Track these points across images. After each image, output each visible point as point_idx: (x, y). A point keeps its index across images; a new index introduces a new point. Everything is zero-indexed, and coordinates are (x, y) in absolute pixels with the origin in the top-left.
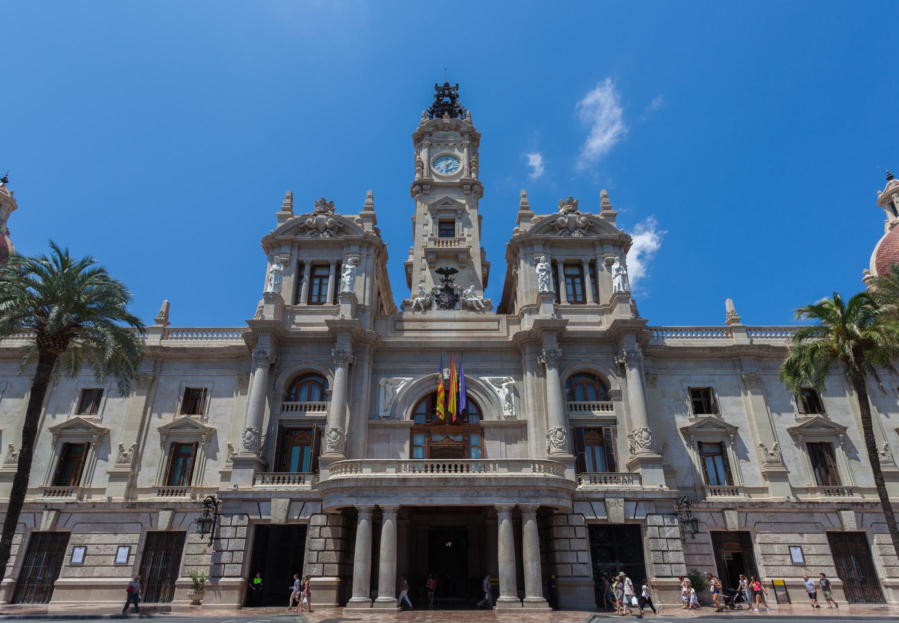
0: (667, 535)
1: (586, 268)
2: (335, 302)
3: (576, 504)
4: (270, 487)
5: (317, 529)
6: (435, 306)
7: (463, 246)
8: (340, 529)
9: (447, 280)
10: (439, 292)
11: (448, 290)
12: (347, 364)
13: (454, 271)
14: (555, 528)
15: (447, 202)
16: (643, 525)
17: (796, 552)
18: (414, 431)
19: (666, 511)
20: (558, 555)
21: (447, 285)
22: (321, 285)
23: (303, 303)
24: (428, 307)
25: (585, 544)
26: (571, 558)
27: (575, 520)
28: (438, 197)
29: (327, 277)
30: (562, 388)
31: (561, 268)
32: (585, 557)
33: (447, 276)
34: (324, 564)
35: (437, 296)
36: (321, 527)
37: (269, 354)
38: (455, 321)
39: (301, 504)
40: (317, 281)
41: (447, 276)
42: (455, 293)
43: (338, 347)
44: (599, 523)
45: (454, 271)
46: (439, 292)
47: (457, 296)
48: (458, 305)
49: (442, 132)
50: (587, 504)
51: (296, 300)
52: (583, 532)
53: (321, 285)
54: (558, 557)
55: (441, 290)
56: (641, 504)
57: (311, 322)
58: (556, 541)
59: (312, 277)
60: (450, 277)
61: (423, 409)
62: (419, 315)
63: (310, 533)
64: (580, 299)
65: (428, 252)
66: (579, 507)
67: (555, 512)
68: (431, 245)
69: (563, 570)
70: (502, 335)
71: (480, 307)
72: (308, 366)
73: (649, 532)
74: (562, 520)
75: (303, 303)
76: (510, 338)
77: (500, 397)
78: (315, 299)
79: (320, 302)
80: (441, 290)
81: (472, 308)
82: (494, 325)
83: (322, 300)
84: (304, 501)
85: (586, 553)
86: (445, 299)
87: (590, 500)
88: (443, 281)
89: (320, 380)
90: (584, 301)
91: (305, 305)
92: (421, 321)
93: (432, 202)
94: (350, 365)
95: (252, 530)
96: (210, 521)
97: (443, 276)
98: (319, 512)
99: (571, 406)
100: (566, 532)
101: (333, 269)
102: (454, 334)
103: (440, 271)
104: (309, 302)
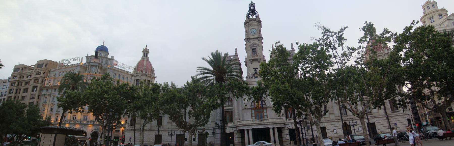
7: (259, 57)
13: (257, 68)
15: (254, 44)
17: (335, 131)
24: (252, 78)
25: (288, 133)
26: (285, 136)
27: (286, 128)
28: (252, 42)
32: (288, 136)
45: (257, 68)
49: (251, 22)
52: (288, 131)
61: (253, 104)
62: (250, 80)
65: (250, 60)
68: (251, 58)
74: (283, 129)
86: (256, 75)
93: (250, 44)
100: (284, 131)
103: (254, 69)
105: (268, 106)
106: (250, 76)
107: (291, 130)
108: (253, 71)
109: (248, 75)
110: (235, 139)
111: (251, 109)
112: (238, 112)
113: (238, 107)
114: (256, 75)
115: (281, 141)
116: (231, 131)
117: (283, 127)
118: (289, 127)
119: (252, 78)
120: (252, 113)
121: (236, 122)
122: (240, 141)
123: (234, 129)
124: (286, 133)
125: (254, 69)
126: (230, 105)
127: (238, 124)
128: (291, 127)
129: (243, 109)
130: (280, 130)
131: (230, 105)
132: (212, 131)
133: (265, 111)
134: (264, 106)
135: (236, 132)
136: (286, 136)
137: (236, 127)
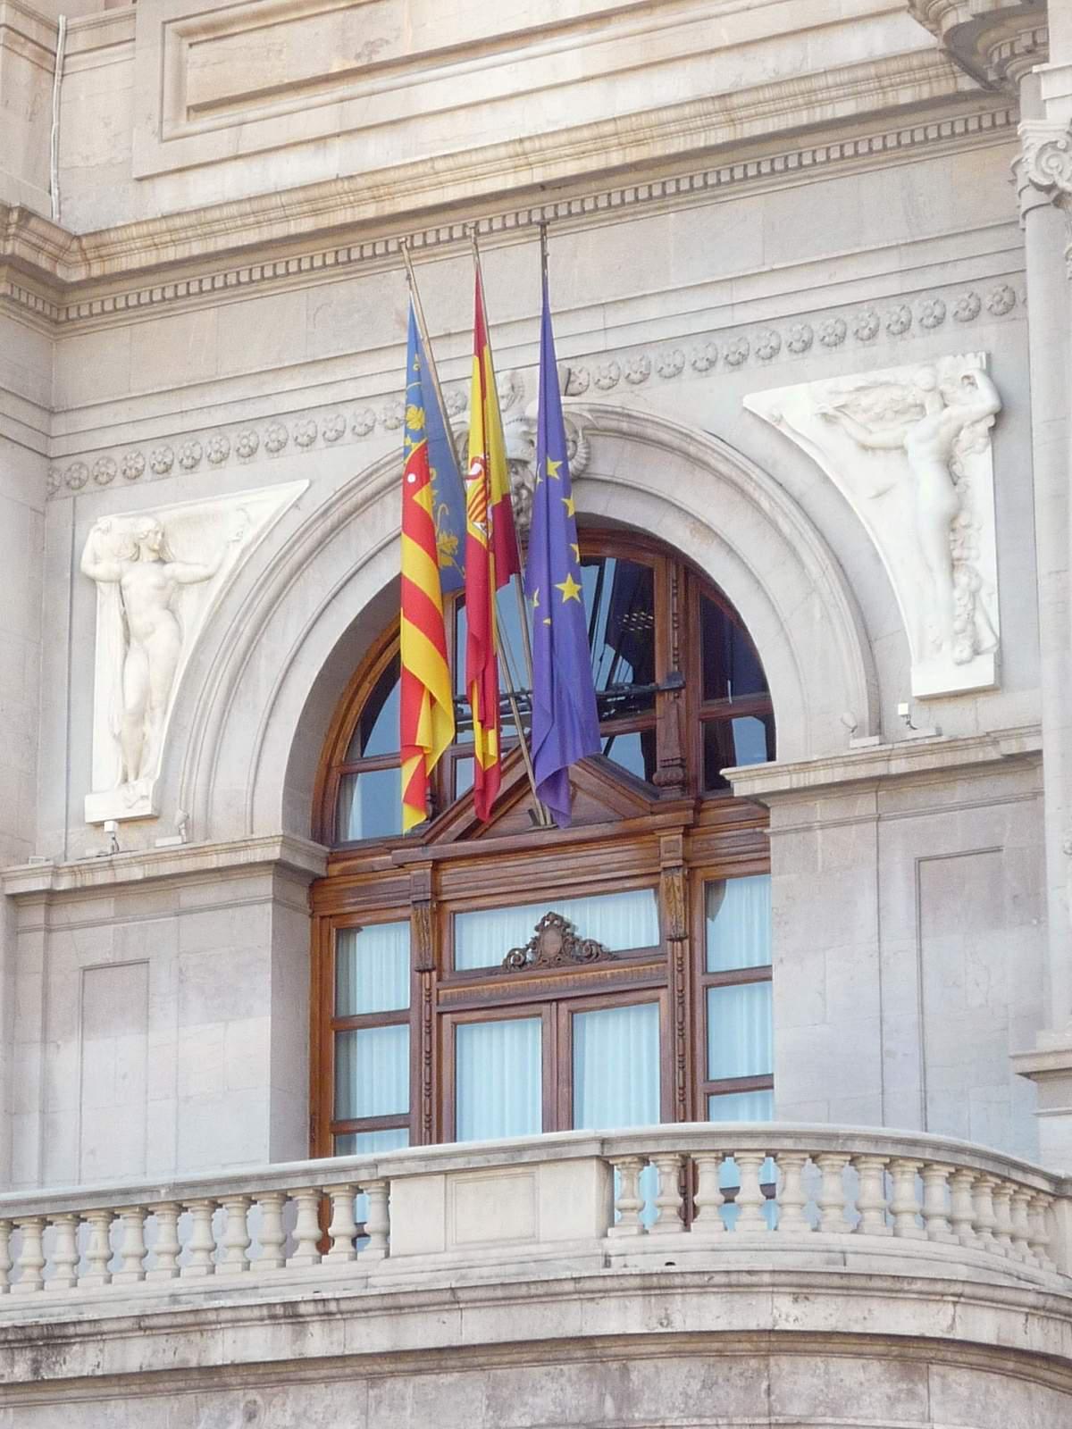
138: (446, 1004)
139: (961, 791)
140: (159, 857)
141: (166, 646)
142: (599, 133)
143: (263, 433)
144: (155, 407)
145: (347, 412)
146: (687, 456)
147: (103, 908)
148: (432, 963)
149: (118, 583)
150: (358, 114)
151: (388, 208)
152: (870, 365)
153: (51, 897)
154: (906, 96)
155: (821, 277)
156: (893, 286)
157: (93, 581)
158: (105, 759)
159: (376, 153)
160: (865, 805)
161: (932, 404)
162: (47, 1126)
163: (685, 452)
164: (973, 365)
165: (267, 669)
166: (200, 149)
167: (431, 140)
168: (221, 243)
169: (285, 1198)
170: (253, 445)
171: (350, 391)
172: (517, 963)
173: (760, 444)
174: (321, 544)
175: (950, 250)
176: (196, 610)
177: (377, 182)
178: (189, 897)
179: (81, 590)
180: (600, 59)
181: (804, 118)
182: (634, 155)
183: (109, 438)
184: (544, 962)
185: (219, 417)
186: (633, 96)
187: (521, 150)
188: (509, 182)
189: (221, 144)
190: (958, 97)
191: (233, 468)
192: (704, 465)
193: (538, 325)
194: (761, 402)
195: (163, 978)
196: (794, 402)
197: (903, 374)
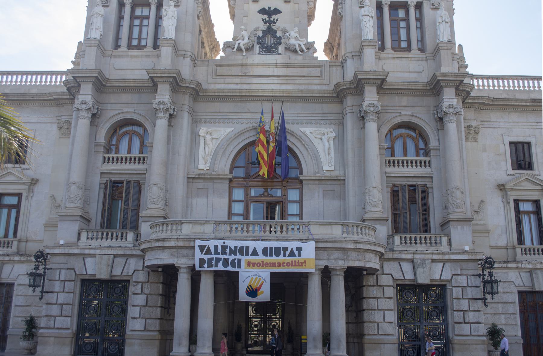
0: (470, 297)
1: (412, 11)
2: (156, 47)
3: (386, 265)
4: (94, 243)
5: (140, 286)
6: (257, 47)
8: (161, 286)
9: (270, 22)
10: (261, 34)
11: (270, 31)
12: (167, 115)
14: (365, 288)
16: (448, 287)
18: (232, 182)
19: (470, 272)
20: (365, 314)
21: (269, 28)
22: (141, 26)
23: (123, 48)
24: (249, 49)
25: (392, 304)
26: (378, 317)
27: (385, 280)
29: (147, 17)
30: (380, 141)
31: (386, 10)
32: (392, 316)
33: (270, 17)
34: (146, 319)
35: (259, 38)
36: (142, 283)
37: (91, 105)
38: (276, 66)
39: (123, 260)
40: (137, 22)
41: (270, 17)
42: (278, 34)
43: (158, 99)
44: (407, 283)
45: (277, 11)
46: (261, 34)
47: (280, 38)
48: (281, 49)
50: (396, 265)
51: (117, 46)
52: (391, 292)
53: (141, 26)
54: (366, 316)
55: (263, 32)
56: (448, 265)
57: (130, 67)
58: (364, 300)
59: (133, 17)
60: (273, 17)
62: (239, 58)
63: (132, 289)
64: (404, 45)
66: (389, 268)
67: (365, 272)
69: (369, 329)
70: (325, 82)
71: (302, 51)
72: (129, 116)
73: (456, 292)
74: (371, 280)
75: (123, 48)
76: (332, 88)
77: (318, 144)
78: (135, 43)
79: (139, 47)
80: (263, 32)
81: (295, 51)
82: (316, 72)
83: (143, 43)
84: (127, 257)
85: (392, 312)
86: (269, 41)
87: (399, 261)
88: (265, 22)
89: (139, 130)
90: (409, 49)
91: (126, 49)
92: (243, 66)
94: (171, 115)
95: (79, 284)
96: (40, 275)
97: (266, 17)
98: (141, 268)
99: (389, 162)
101: (153, 8)
102: (276, 81)
103: (263, 11)
104: (130, 47)
105: (308, 170)
106: (243, 43)
107: (407, 290)
108: (258, 23)
109: (234, 39)
110: (133, 312)
111: (232, 182)
112: (167, 191)
113: (167, 164)
114: (269, 41)
115: (356, 337)
116: (117, 271)
117: (372, 272)
118: (398, 275)
119: (249, 49)
120: (231, 201)
121: (144, 227)
122: (155, 325)
123: (133, 264)
124: (384, 304)
125: (263, 11)
126: (136, 153)
127: (153, 236)
128: (409, 276)
129: (191, 179)
130: (356, 280)
131: (136, 153)
132: (30, 268)
133: (293, 195)
134: (293, 173)
135: (141, 277)
136: (384, 316)
137: (143, 257)
138: (247, 201)
139: (329, 182)
140: (213, 175)
141: (211, 147)
142: (283, 91)
143: (226, 121)
144: (210, 114)
145: (240, 120)
146: (292, 134)
147: (201, 181)
148: (247, 194)
149: (204, 137)
150: (243, 81)
151: (251, 94)
152: (317, 127)
153: (194, 178)
154: (326, 95)
155: (310, 115)
156: (320, 118)
157: (200, 136)
158: (201, 161)
159: (245, 87)
160: (316, 182)
161: (326, 134)
162: (192, 210)
163: (293, 134)
164: (332, 130)
165: (228, 152)
166: (218, 81)
167: (254, 87)
168: (224, 94)
169: (357, 227)
170: (226, 122)
171: (241, 117)
172: (260, 196)
173: (301, 135)
174: (237, 137)
175: (328, 115)
176: (216, 143)
177: (250, 91)
178: (215, 181)
179: (197, 137)
180: (280, 82)
181: (312, 95)
182: (287, 95)
183: (202, 117)
184: (265, 196)
185: (220, 117)
186: (284, 87)
187: (272, 91)
188: (269, 95)
189: (222, 81)
190: (333, 97)
191: (222, 124)
192: (294, 136)
193: (270, 115)
194: (302, 129)
195: (211, 191)
196: (308, 130)
197: (322, 129)
